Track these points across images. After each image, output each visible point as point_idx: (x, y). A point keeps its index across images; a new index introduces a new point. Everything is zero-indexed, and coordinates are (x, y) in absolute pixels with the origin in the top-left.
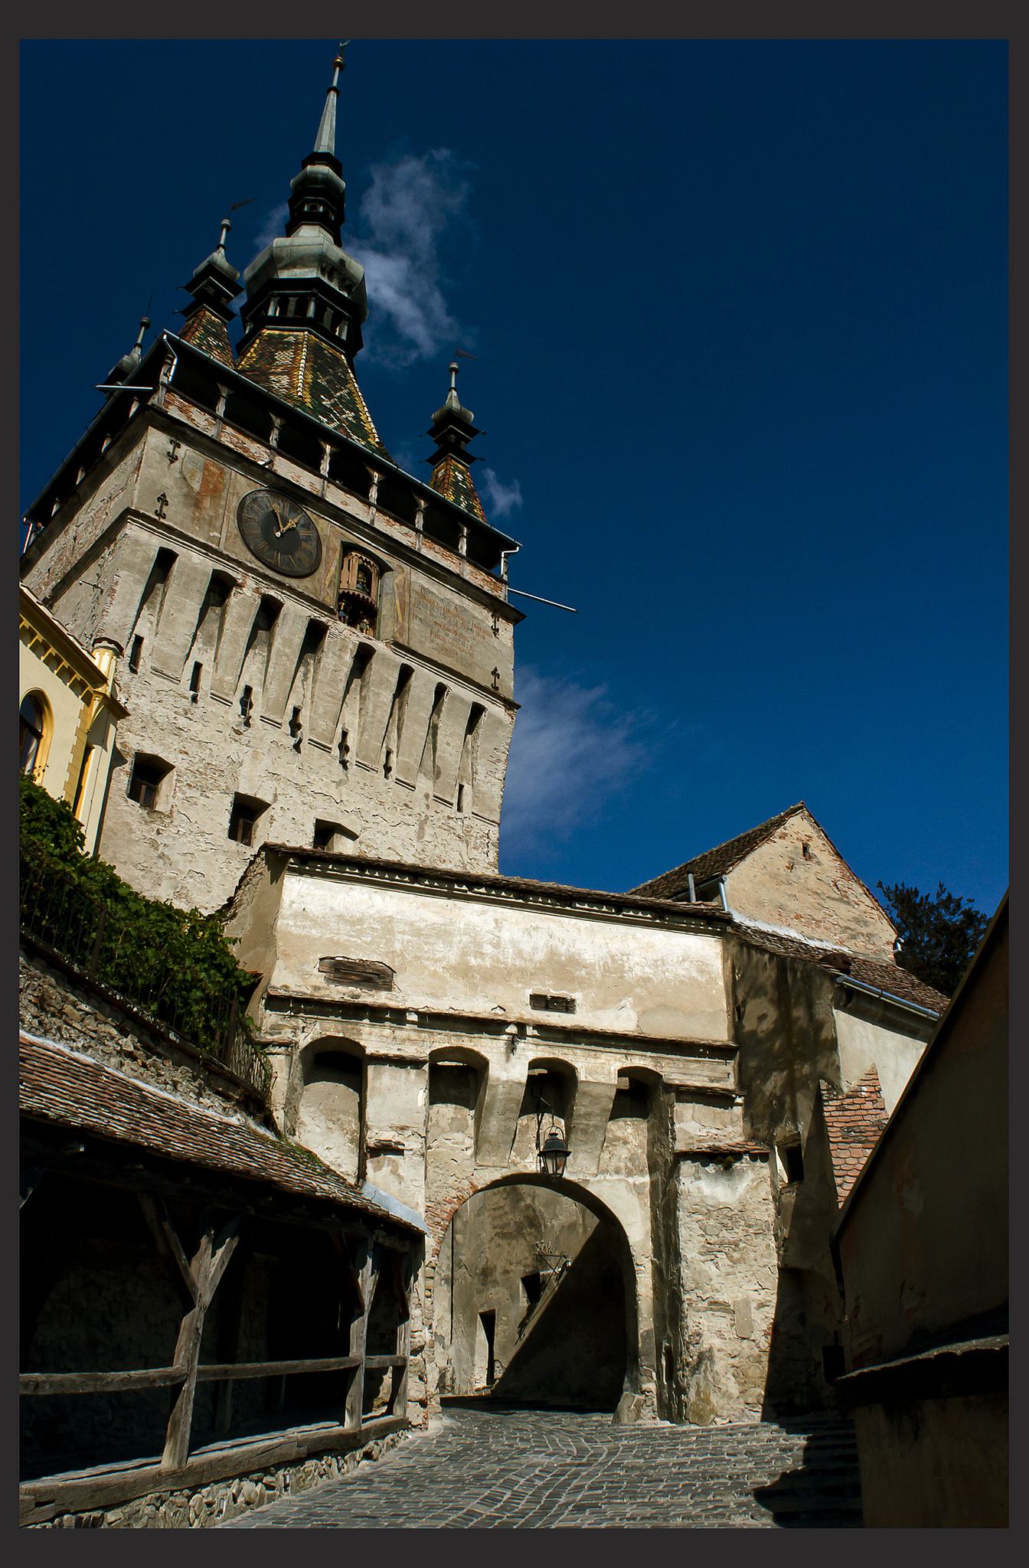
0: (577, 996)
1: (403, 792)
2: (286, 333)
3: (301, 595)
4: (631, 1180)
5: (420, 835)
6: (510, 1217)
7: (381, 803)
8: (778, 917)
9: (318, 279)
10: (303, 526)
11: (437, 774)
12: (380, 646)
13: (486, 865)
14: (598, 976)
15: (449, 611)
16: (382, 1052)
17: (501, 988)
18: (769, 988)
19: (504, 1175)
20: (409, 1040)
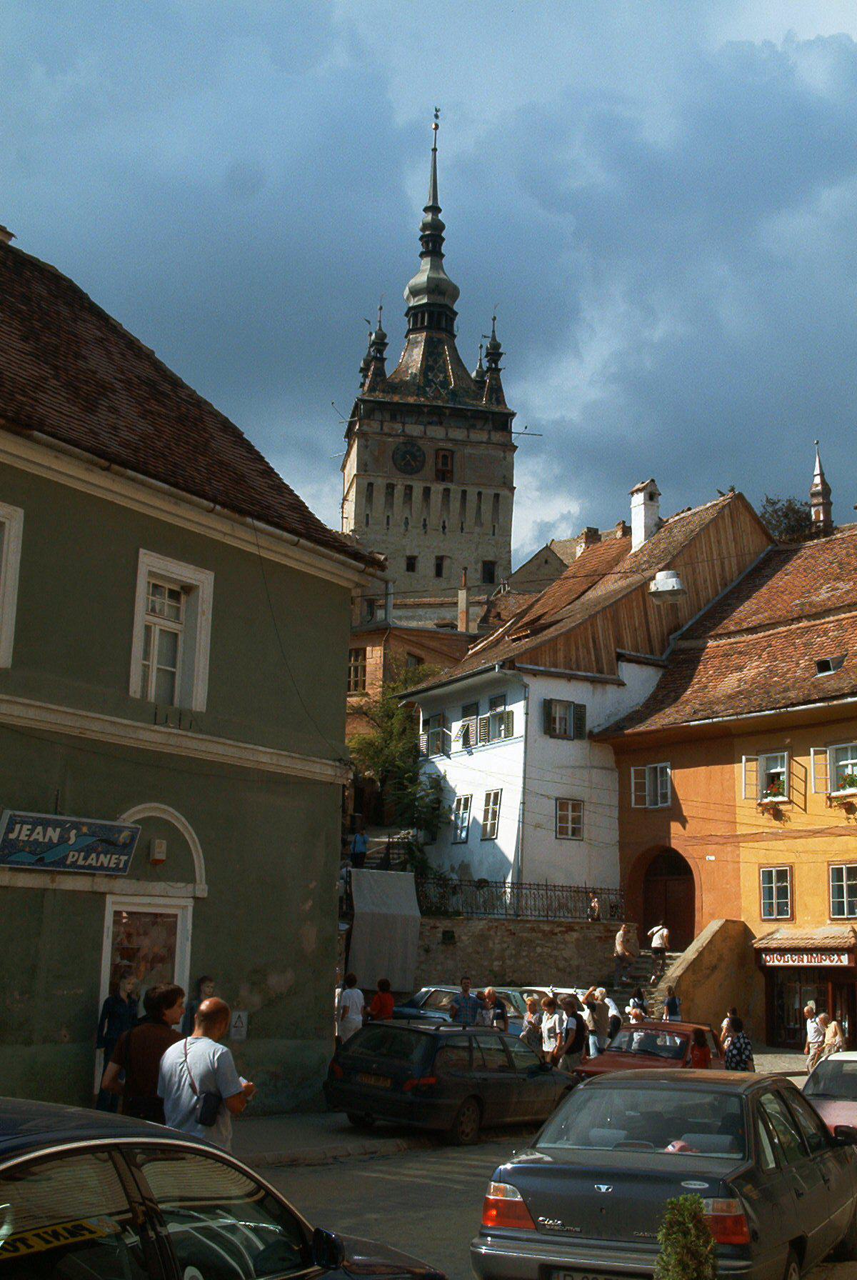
2: (418, 335)
5: (477, 549)
11: (482, 525)
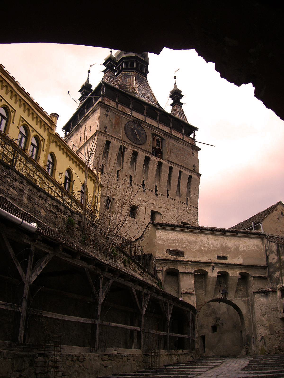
0: (228, 256)
1: (172, 201)
2: (129, 72)
3: (143, 149)
4: (242, 299)
5: (177, 213)
6: (208, 311)
7: (167, 205)
8: (276, 232)
9: (136, 56)
10: (141, 130)
11: (180, 195)
12: (163, 161)
13: (195, 219)
14: (233, 250)
15: (181, 150)
16: (183, 271)
17: (210, 255)
18: (275, 251)
19: (213, 299)
20: (189, 268)
